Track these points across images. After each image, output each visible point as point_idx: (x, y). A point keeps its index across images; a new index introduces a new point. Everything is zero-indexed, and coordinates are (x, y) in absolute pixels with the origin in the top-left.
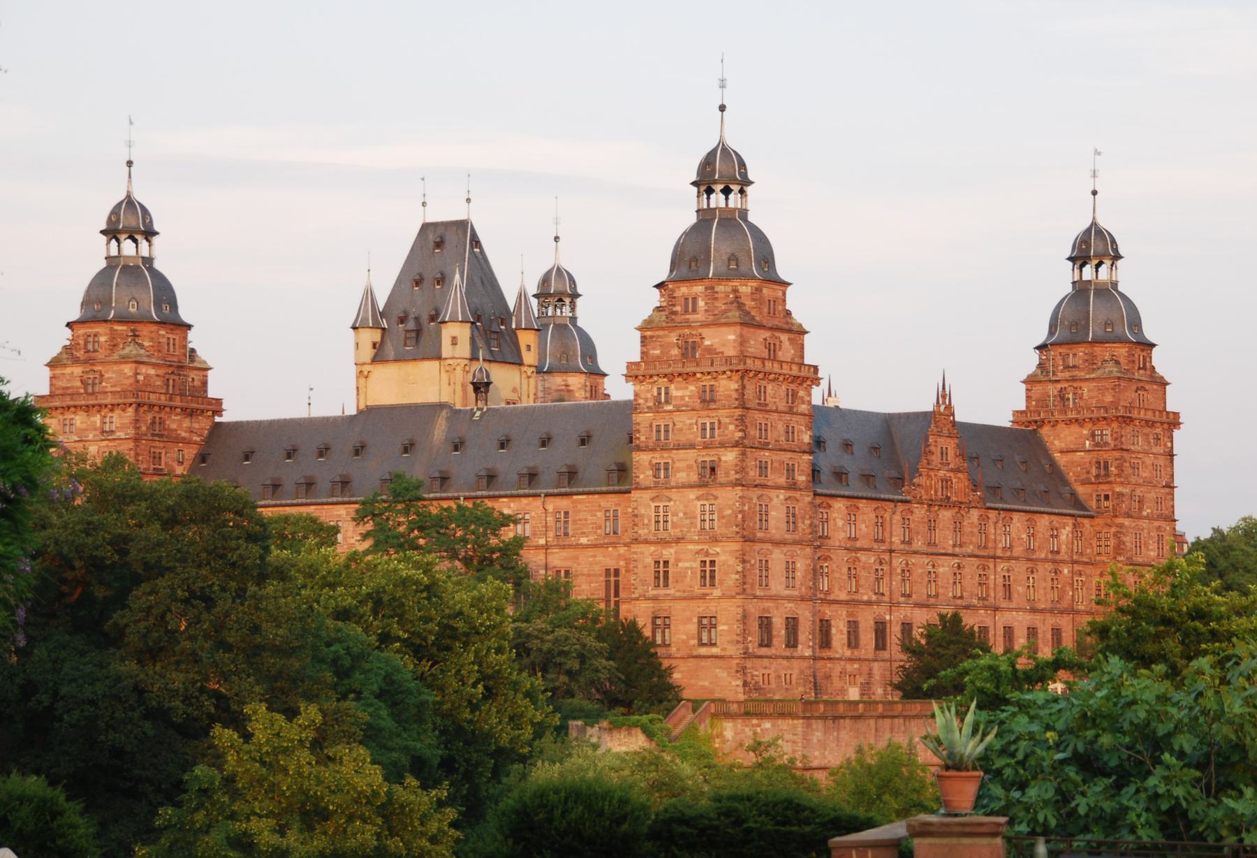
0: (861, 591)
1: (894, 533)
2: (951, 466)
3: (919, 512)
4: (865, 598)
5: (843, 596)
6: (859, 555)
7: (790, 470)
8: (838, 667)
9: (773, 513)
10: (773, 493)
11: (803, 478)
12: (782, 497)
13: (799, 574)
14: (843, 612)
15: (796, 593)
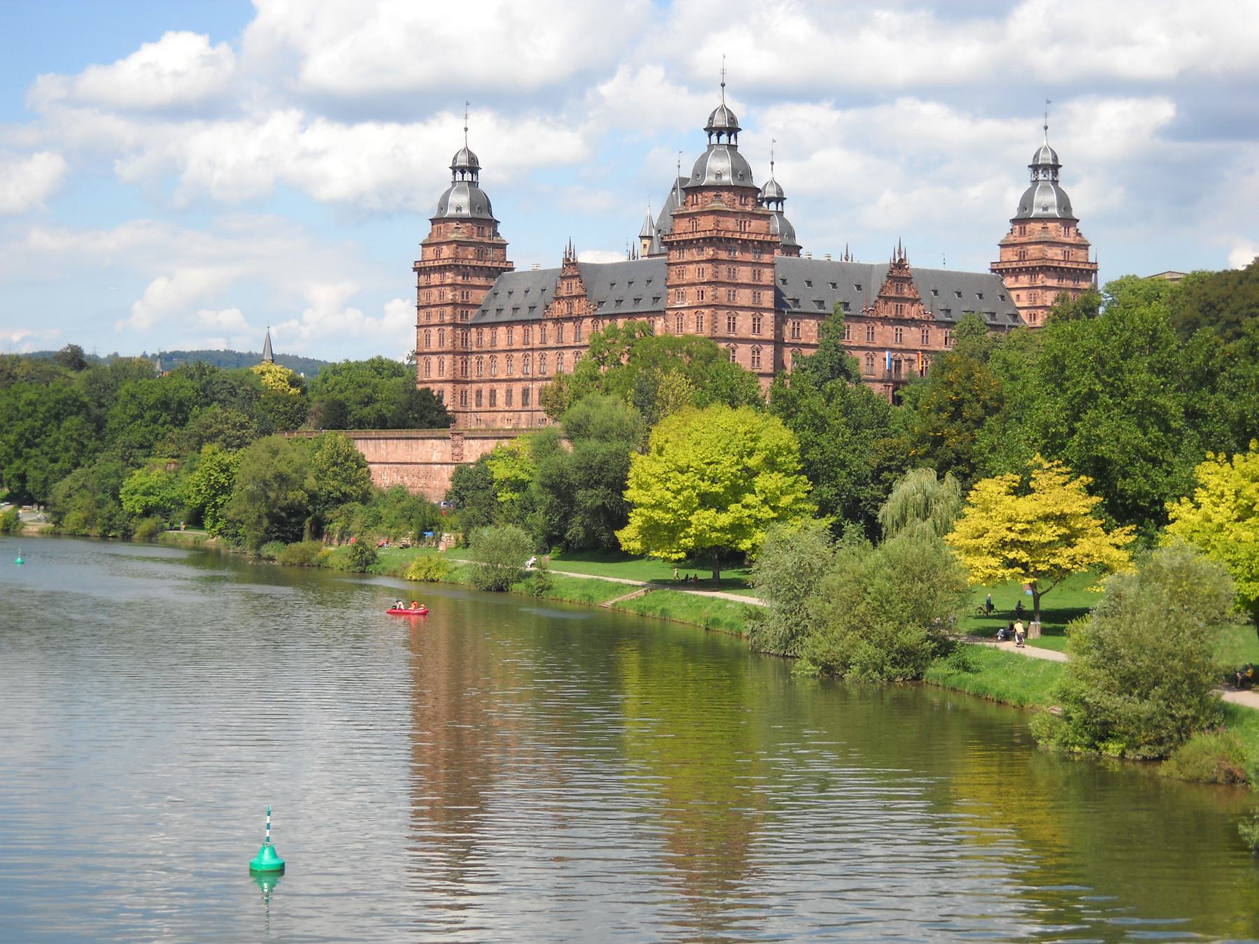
0: (514, 372)
1: (535, 338)
2: (574, 294)
3: (550, 325)
4: (517, 377)
5: (504, 377)
6: (513, 353)
7: (442, 315)
8: (500, 415)
9: (431, 338)
10: (431, 329)
11: (448, 318)
12: (437, 329)
13: (445, 368)
14: (504, 385)
15: (444, 378)
